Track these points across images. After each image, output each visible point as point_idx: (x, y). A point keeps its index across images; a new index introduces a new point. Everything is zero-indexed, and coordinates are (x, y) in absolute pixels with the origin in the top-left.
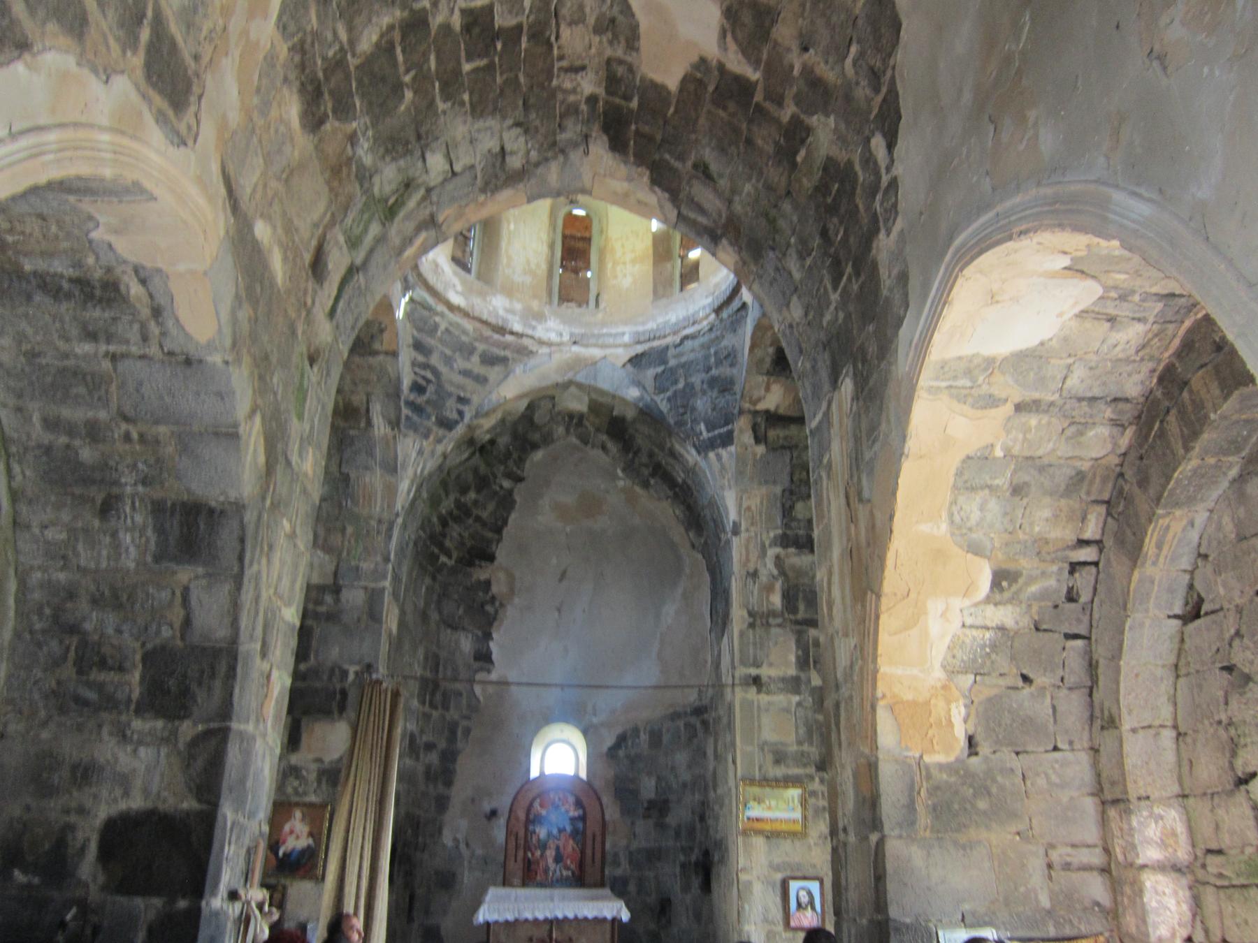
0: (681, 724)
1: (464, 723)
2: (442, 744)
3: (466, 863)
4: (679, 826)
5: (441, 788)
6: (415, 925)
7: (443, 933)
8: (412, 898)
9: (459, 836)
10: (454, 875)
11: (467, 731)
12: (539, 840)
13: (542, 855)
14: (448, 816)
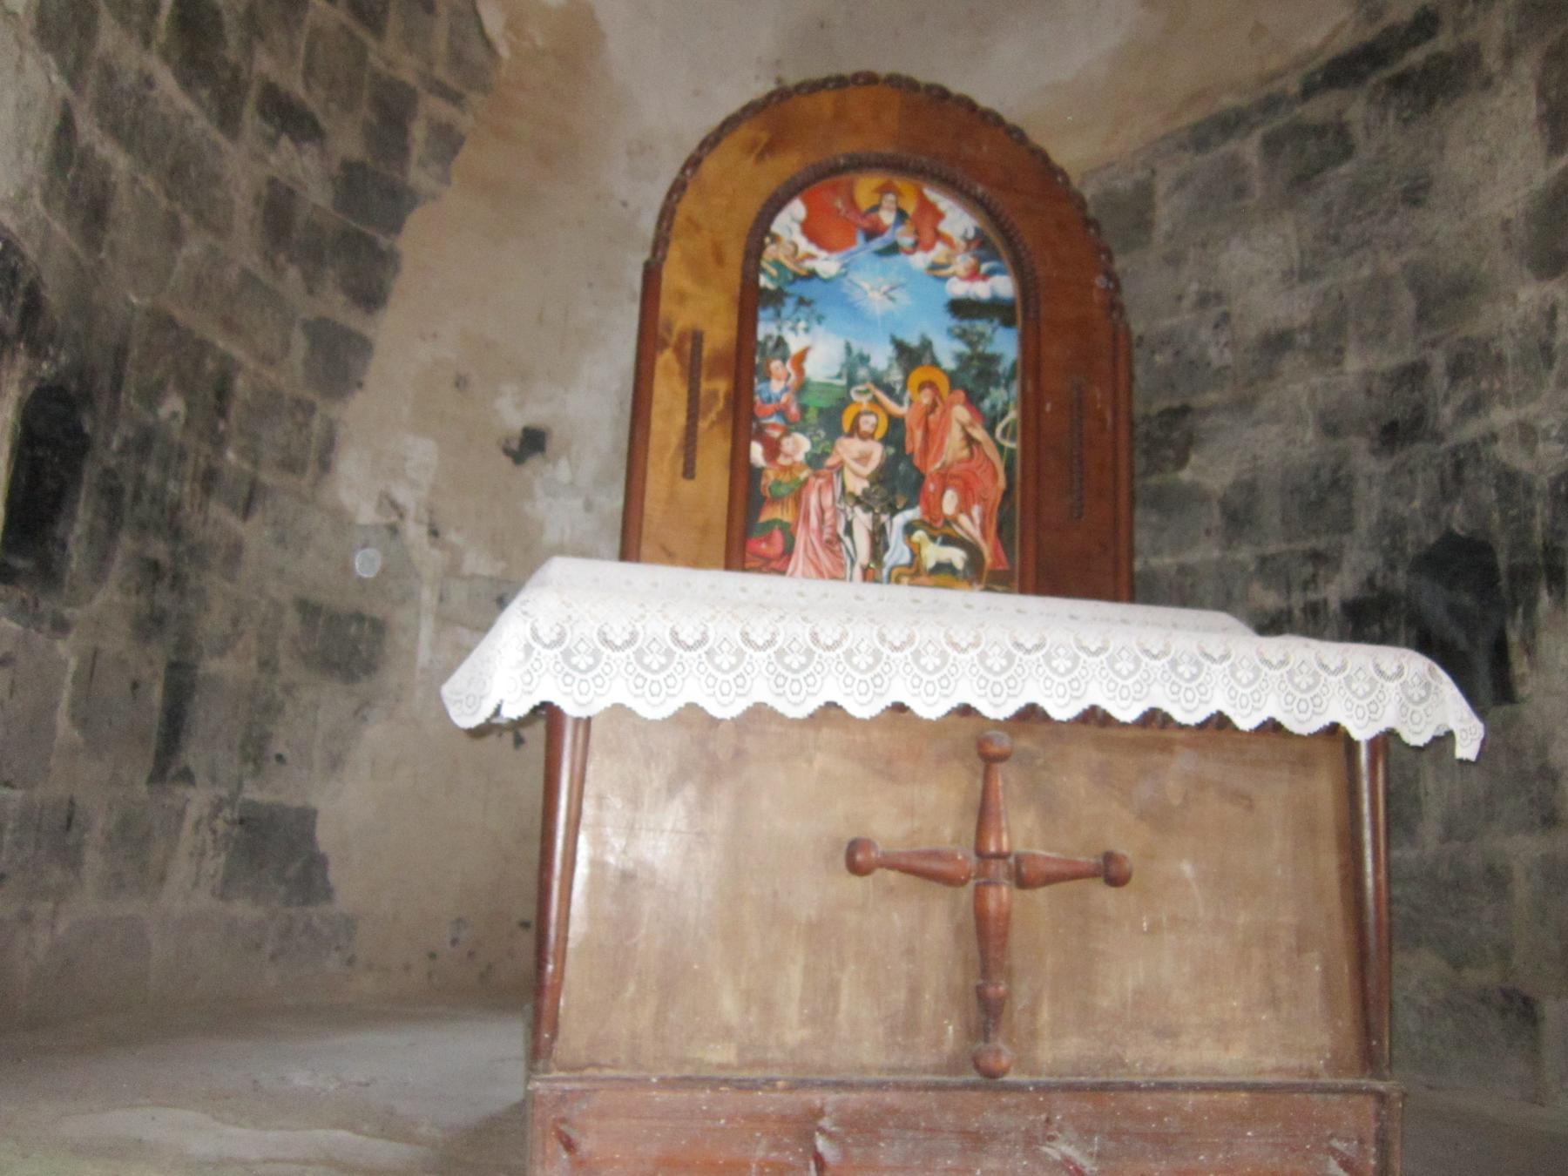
0: (1249, 148)
1: (434, 107)
2: (348, 141)
3: (427, 596)
4: (1249, 488)
5: (335, 305)
6: (197, 800)
7: (325, 837)
8: (181, 687)
9: (402, 495)
10: (379, 628)
11: (448, 141)
12: (802, 387)
13: (815, 461)
14: (357, 413)
